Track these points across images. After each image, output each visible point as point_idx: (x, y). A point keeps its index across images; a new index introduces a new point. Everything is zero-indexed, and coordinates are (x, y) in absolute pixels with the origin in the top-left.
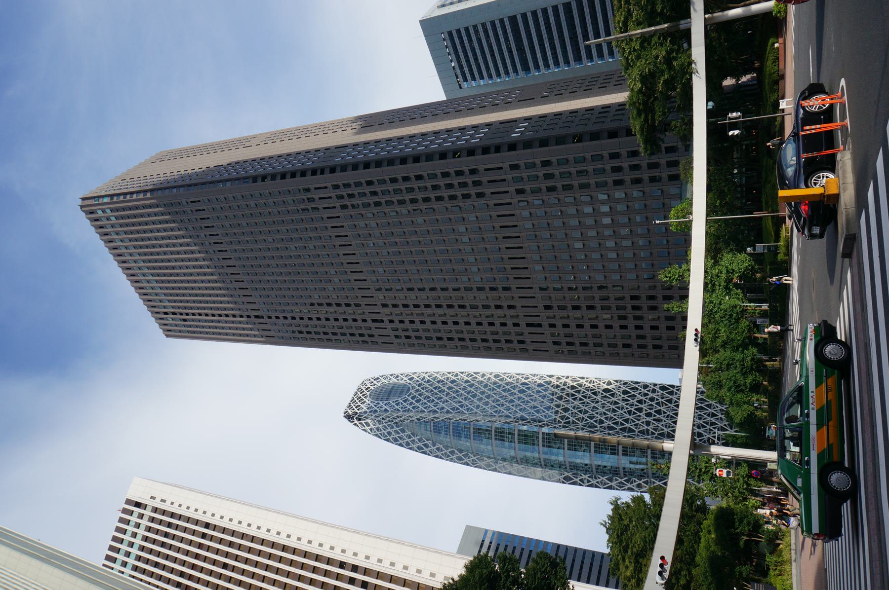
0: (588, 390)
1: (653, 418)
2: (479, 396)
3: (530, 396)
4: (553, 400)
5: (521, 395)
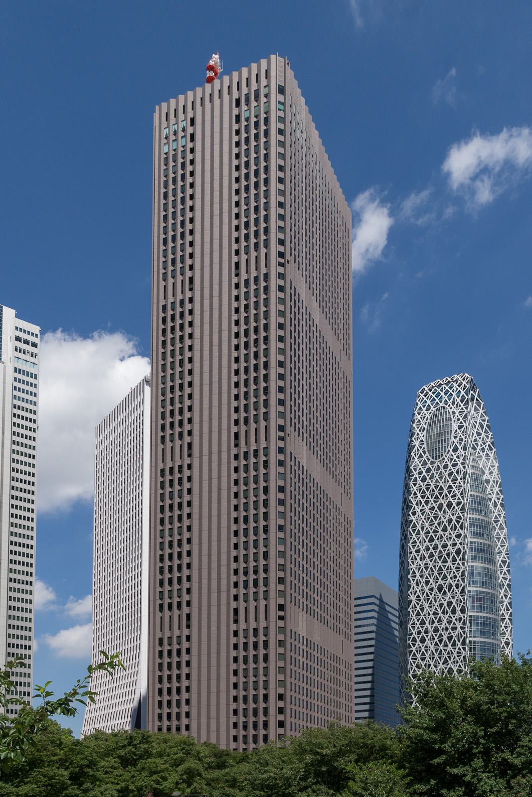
3: (435, 599)
5: (435, 589)
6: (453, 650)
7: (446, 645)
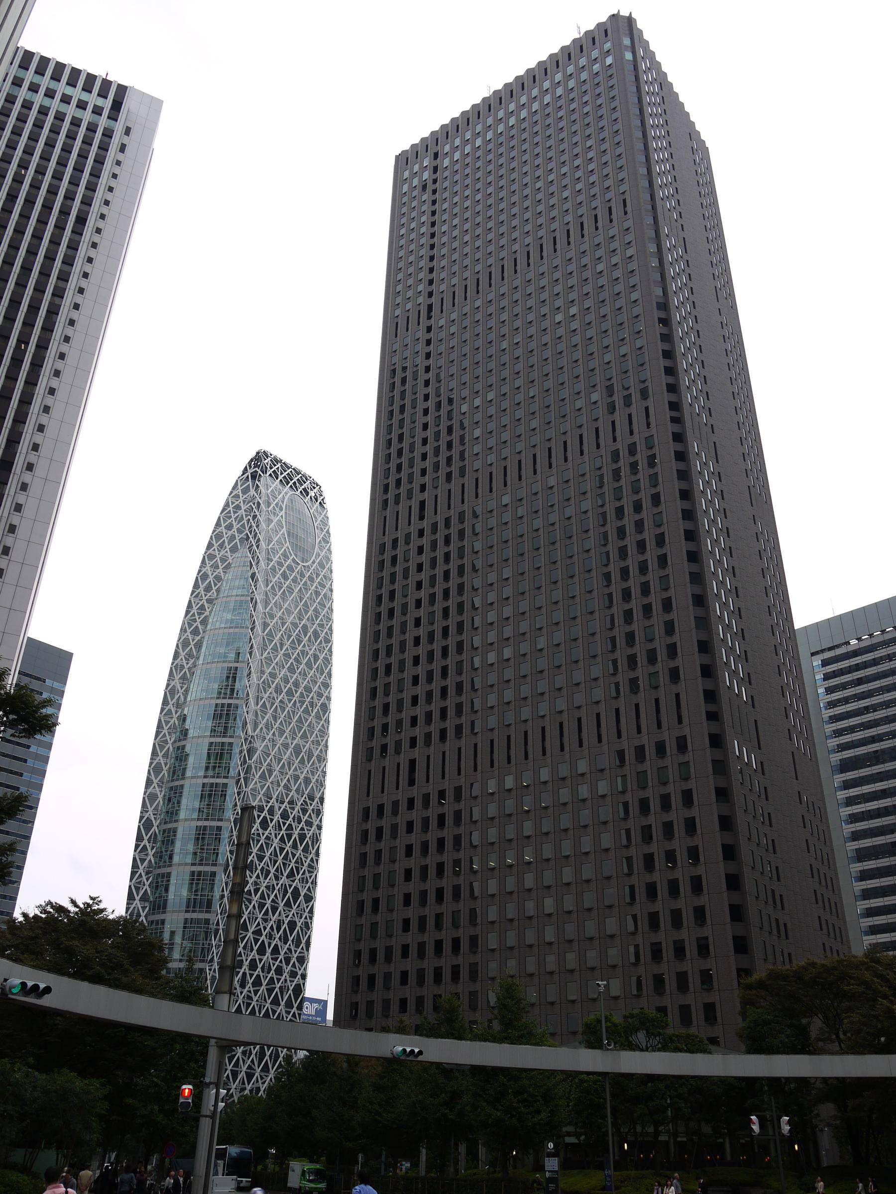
0: (296, 862)
1: (248, 972)
2: (292, 677)
3: (289, 763)
4: (282, 802)
6: (303, 859)
7: (295, 846)
